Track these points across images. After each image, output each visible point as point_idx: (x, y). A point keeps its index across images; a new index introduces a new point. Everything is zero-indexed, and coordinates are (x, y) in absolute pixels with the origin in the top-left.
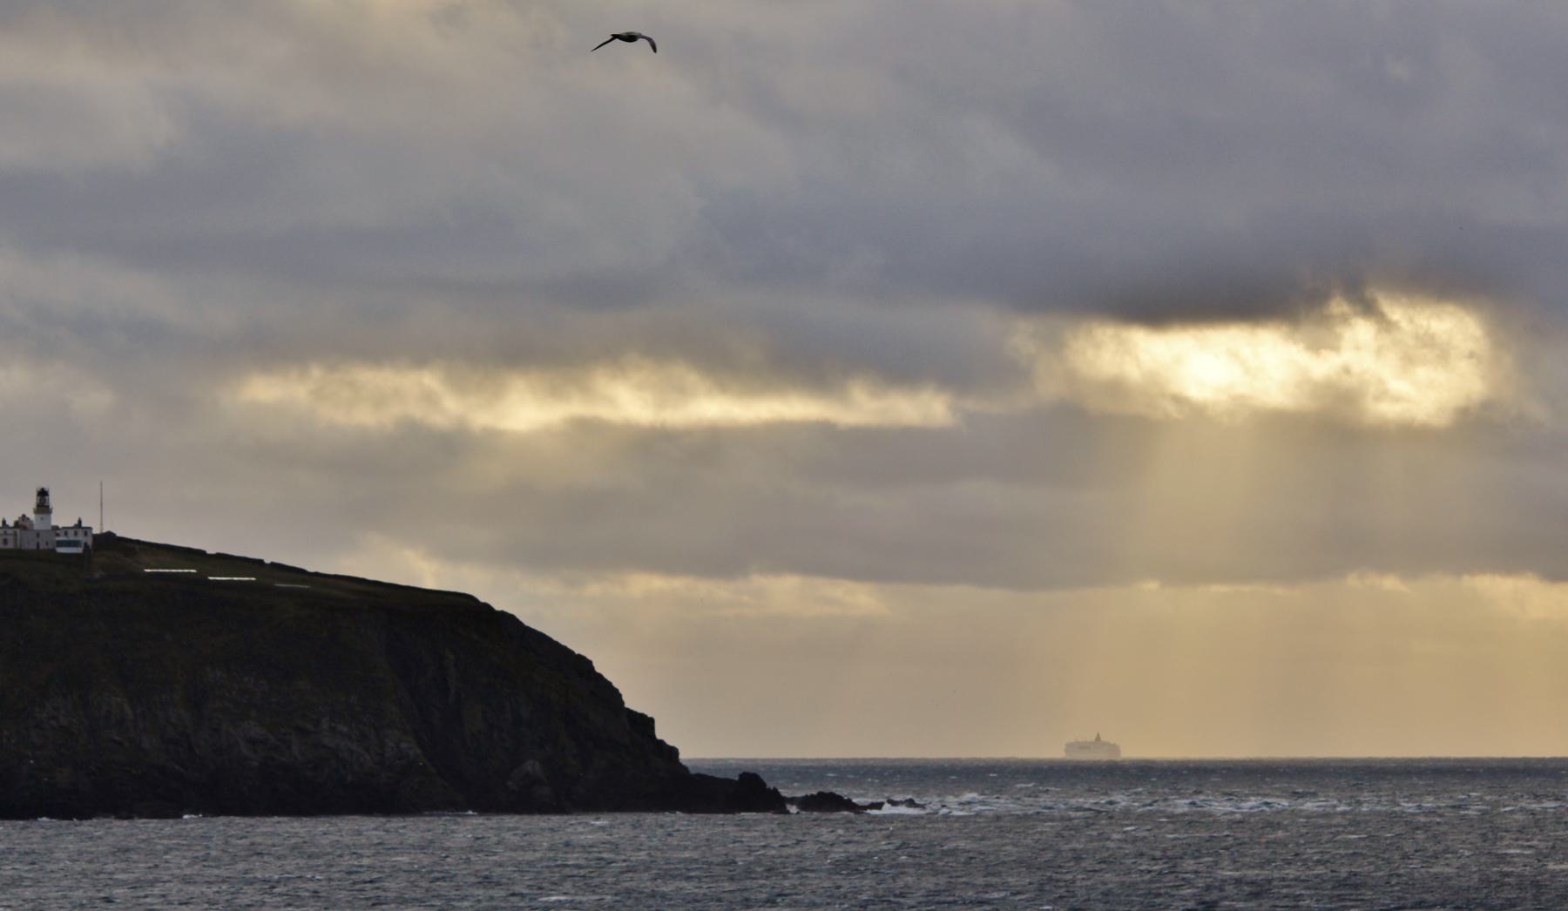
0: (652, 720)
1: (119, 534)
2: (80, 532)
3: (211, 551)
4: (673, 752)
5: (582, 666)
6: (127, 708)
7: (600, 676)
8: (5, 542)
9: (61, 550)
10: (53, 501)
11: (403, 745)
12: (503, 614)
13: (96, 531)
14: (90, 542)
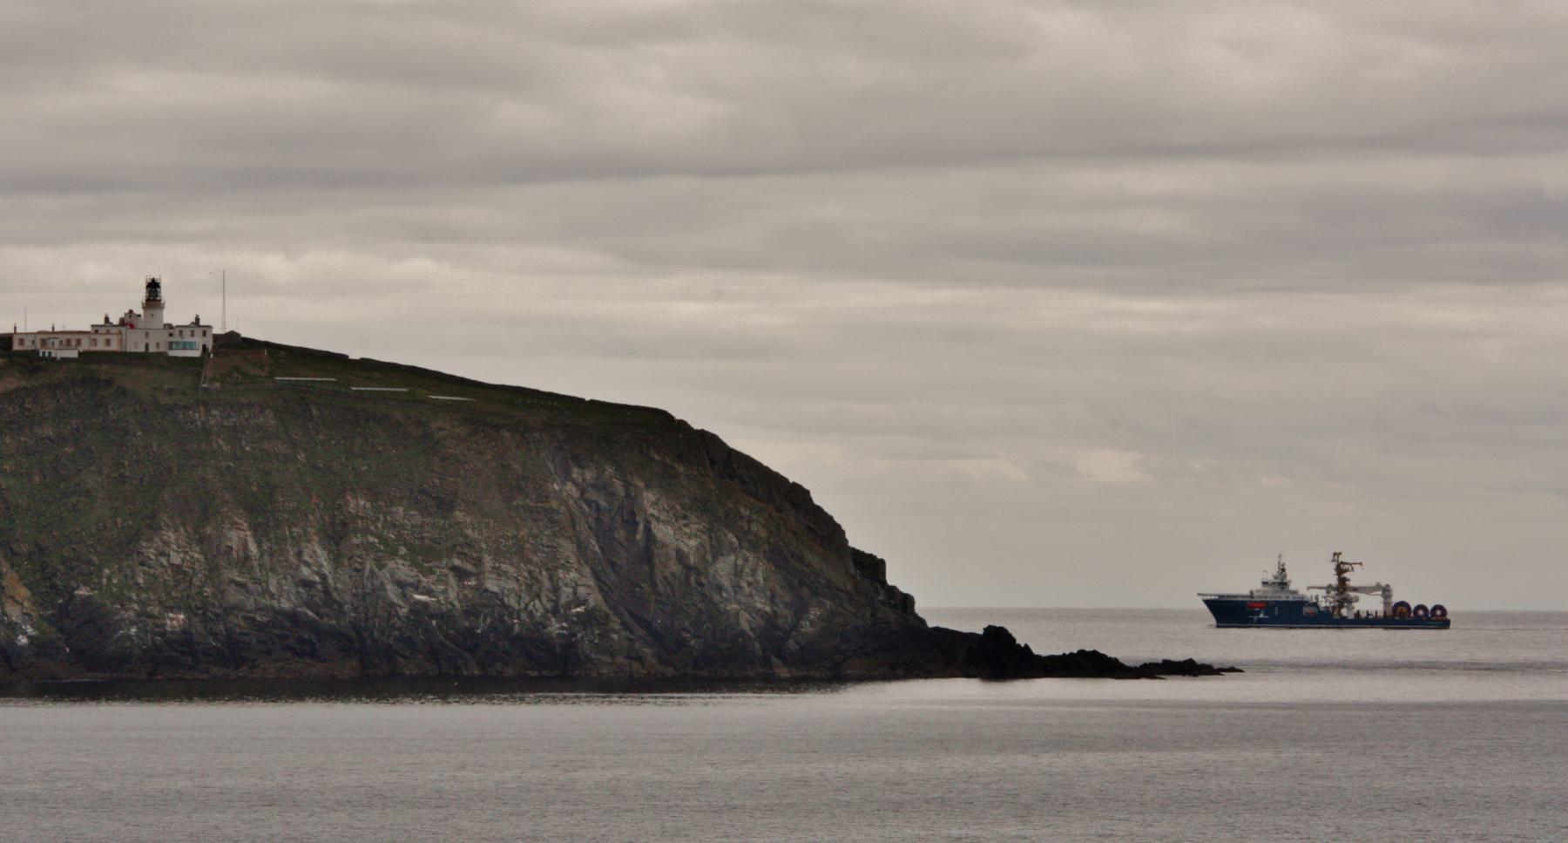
0: (882, 562)
2: (198, 332)
3: (355, 355)
4: (907, 601)
5: (797, 496)
6: (253, 548)
7: (819, 509)
8: (108, 342)
9: (172, 353)
10: (165, 293)
11: (582, 591)
12: (703, 433)
13: (217, 330)
14: (210, 346)
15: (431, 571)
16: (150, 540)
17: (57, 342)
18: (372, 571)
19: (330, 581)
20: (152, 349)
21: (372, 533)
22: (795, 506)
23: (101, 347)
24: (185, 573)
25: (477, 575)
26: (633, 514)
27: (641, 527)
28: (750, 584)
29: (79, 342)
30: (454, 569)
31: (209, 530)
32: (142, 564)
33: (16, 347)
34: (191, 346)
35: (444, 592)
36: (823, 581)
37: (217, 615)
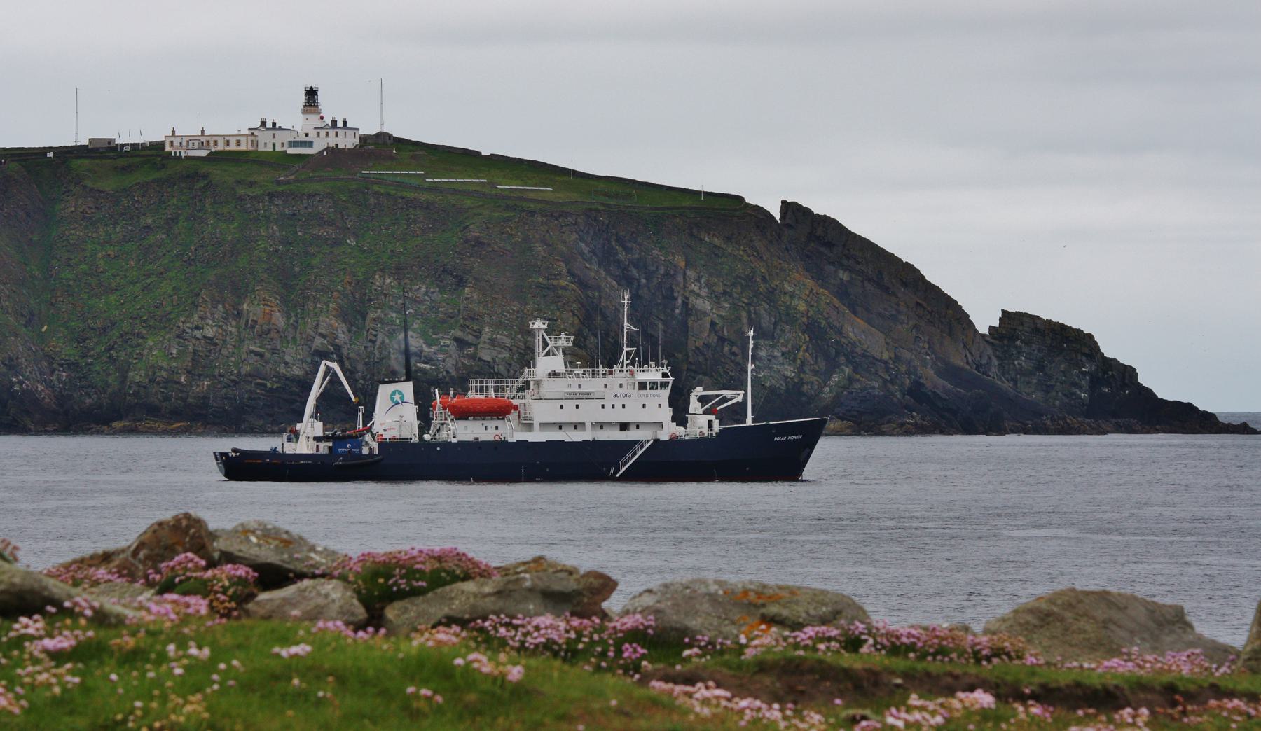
0: (1090, 336)
1: (397, 133)
6: (279, 320)
9: (291, 151)
10: (321, 98)
13: (371, 130)
15: (436, 342)
16: (190, 316)
17: (196, 143)
18: (383, 342)
19: (345, 351)
20: (278, 148)
21: (391, 307)
22: (905, 284)
23: (233, 147)
24: (216, 345)
25: (476, 345)
26: (672, 290)
27: (680, 301)
28: (783, 354)
29: (216, 143)
30: (456, 340)
31: (245, 306)
32: (179, 337)
33: (167, 148)
34: (310, 144)
35: (444, 361)
36: (858, 350)
37: (233, 381)
